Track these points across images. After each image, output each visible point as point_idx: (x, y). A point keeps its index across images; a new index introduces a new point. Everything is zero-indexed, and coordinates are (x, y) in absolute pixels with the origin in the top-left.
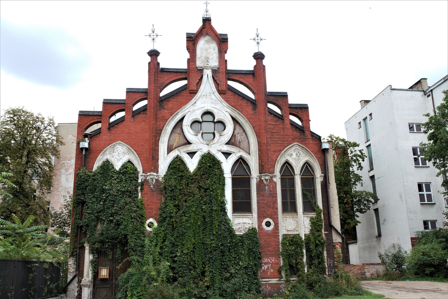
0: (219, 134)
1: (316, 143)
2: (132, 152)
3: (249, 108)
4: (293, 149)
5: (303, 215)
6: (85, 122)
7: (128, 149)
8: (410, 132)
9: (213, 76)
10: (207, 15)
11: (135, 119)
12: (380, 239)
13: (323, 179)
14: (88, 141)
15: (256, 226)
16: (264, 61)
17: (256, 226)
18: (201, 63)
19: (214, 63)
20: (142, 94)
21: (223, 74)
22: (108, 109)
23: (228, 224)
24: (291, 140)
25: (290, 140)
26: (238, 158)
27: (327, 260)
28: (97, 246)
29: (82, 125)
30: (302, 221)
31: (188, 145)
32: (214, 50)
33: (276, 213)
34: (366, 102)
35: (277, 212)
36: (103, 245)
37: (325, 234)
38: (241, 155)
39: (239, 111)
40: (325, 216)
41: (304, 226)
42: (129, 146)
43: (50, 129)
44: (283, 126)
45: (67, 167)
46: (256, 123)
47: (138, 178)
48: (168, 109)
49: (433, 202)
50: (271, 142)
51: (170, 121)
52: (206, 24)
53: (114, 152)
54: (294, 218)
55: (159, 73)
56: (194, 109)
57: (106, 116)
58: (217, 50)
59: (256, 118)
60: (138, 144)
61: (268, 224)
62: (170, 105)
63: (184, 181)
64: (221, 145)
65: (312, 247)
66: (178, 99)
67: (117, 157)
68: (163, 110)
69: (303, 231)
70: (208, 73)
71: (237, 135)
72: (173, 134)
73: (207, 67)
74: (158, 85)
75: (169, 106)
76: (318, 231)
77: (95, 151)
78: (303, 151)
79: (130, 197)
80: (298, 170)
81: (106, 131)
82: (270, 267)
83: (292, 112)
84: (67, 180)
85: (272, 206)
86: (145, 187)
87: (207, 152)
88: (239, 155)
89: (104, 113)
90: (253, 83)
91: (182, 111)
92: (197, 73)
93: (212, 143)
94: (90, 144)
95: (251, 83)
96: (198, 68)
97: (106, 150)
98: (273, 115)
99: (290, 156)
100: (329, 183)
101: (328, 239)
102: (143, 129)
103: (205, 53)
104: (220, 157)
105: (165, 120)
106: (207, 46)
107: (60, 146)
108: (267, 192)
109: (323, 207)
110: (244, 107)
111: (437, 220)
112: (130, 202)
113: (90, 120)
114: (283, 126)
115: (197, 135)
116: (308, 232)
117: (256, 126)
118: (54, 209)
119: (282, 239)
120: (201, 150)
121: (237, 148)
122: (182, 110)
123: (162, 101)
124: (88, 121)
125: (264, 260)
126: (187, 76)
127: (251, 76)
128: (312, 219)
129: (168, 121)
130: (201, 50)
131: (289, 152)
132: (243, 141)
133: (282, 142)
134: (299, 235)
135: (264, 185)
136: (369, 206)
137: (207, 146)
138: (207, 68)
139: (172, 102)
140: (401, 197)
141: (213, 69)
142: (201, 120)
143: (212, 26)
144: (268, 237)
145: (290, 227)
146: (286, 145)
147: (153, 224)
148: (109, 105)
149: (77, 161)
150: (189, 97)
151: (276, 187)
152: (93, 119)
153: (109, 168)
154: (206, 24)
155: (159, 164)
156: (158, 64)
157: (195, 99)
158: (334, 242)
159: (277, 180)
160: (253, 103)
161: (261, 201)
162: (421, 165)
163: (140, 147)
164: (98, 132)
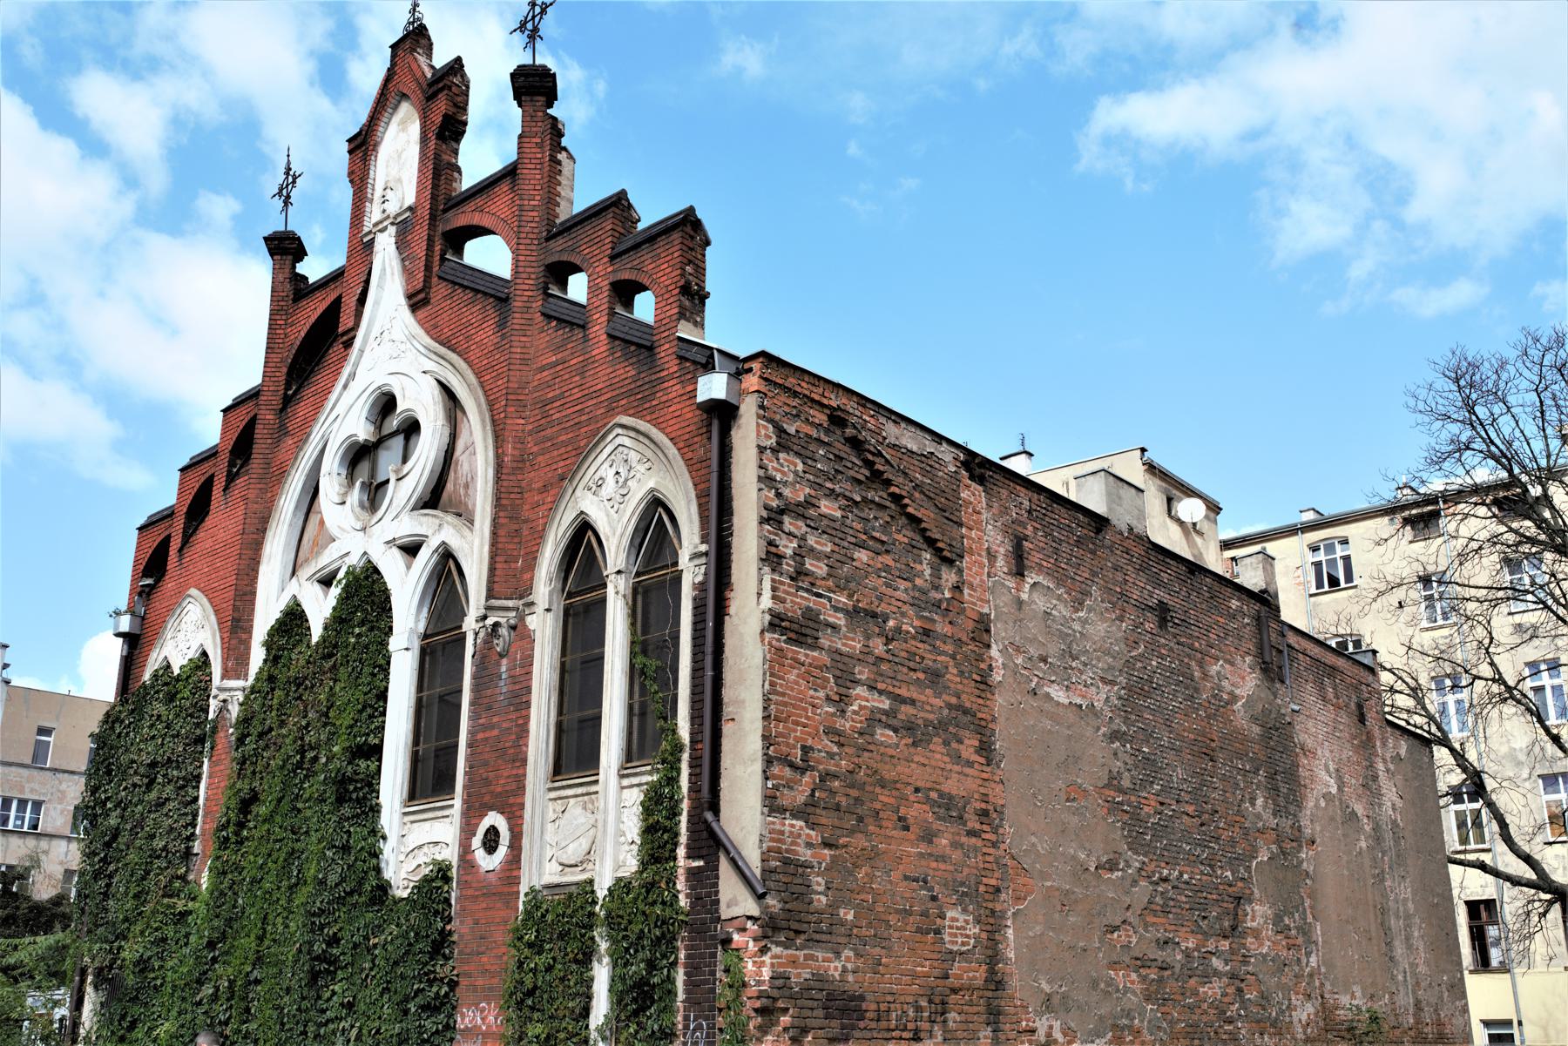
10: (413, 22)
15: (450, 854)
17: (450, 854)
24: (602, 411)
27: (686, 1018)
37: (692, 874)
70: (386, 245)
71: (461, 458)
78: (640, 447)
96: (365, 240)
101: (698, 898)
108: (504, 687)
114: (581, 359)
116: (631, 865)
133: (570, 436)
135: (498, 657)
137: (361, 533)
138: (380, 227)
141: (399, 219)
144: (484, 905)
158: (725, 913)
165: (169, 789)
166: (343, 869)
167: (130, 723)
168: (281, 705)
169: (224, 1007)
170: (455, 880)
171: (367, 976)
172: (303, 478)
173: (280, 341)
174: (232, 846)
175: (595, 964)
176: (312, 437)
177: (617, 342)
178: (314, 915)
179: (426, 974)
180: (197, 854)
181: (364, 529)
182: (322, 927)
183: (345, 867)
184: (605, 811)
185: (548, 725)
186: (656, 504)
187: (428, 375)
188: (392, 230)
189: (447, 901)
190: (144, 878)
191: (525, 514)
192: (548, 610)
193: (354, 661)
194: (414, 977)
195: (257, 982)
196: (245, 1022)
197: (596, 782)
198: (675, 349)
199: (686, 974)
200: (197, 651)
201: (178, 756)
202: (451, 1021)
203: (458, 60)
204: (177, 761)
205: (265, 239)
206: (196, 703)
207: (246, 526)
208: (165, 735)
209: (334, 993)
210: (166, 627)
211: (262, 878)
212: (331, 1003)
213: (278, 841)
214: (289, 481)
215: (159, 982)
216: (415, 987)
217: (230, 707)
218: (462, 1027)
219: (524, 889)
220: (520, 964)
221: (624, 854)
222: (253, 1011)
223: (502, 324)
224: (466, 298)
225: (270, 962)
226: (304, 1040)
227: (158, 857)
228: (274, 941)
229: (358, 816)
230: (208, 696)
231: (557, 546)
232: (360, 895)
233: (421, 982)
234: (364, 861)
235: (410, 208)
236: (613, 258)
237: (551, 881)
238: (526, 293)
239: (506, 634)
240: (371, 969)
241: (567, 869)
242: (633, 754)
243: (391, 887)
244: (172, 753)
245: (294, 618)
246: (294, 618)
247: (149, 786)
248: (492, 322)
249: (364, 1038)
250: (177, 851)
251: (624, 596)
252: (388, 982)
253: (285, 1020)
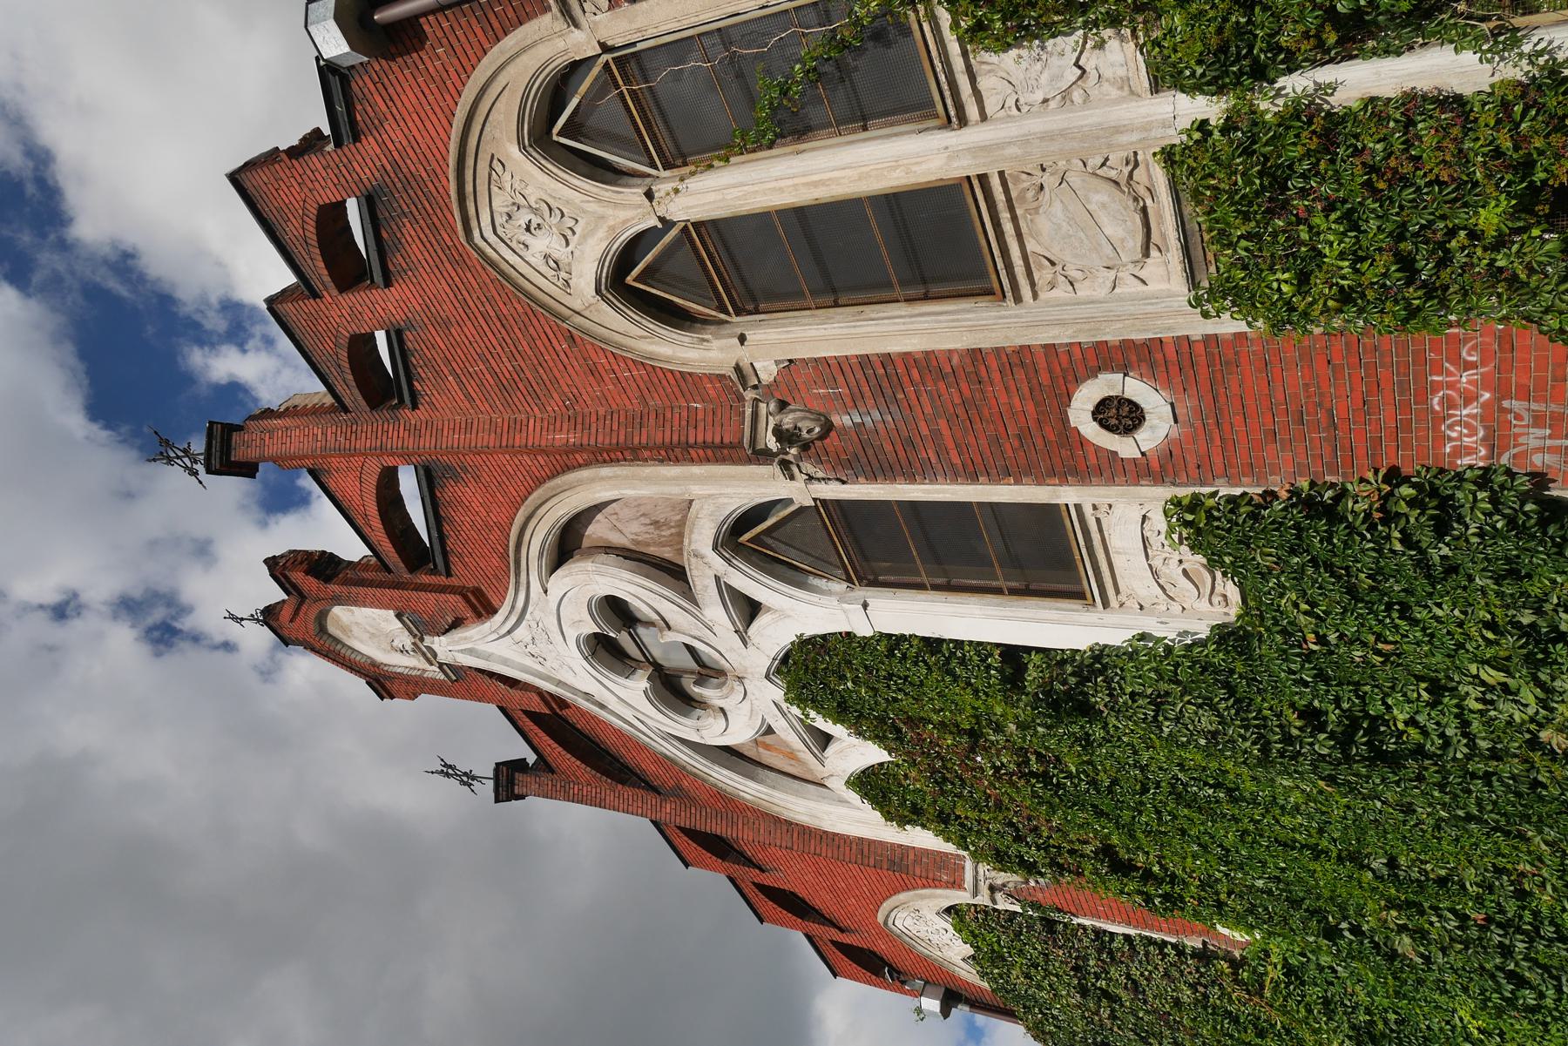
5: (963, 121)
9: (444, 634)
15: (1155, 497)
35: (998, 351)
38: (715, 548)
54: (1022, 197)
82: (1534, 406)
85: (963, 385)
88: (718, 564)
96: (454, 678)
98: (416, 383)
99: (563, 274)
108: (872, 417)
125: (1459, 452)
128: (976, 33)
135: (833, 434)
137: (745, 681)
138: (429, 655)
165: (1114, 972)
166: (1189, 702)
167: (1041, 1012)
168: (976, 806)
169: (1434, 919)
170: (1198, 490)
171: (1378, 653)
172: (716, 768)
173: (594, 790)
174: (1177, 889)
175: (1340, 100)
176: (667, 753)
177: (391, 267)
178: (1265, 750)
179: (1372, 528)
180: (1204, 943)
181: (740, 679)
182: (1288, 739)
183: (1187, 698)
184: (1025, 141)
185: (911, 316)
187: (549, 586)
188: (428, 640)
189: (1231, 500)
190: (1235, 1020)
191: (635, 406)
192: (742, 339)
193: (889, 687)
194: (1379, 551)
195: (1392, 863)
196: (1463, 887)
197: (983, 178)
198: (351, 146)
201: (1070, 956)
202: (1468, 474)
203: (266, 561)
204: (1077, 958)
205: (497, 801)
206: (1002, 926)
207: (784, 845)
208: (1045, 970)
209: (1411, 722)
210: (928, 956)
211: (1221, 846)
212: (1431, 726)
213: (1160, 819)
214: (724, 786)
215: (1392, 1017)
216: (1398, 547)
218: (1483, 452)
219: (1197, 327)
220: (1345, 297)
221: (1106, 86)
222: (1443, 872)
224: (452, 533)
225: (1358, 840)
226: (1500, 779)
227: (1205, 996)
228: (1321, 831)
229: (1108, 681)
230: (995, 910)
231: (653, 334)
232: (1232, 672)
233: (1388, 538)
234: (1177, 665)
235: (399, 616)
236: (315, 295)
237: (1180, 267)
238: (401, 435)
239: (791, 416)
240: (1364, 644)
241: (1155, 237)
243: (1224, 626)
244: (1067, 963)
245: (869, 784)
246: (869, 784)
247: (1113, 999)
248: (456, 488)
249: (1503, 654)
250: (1198, 971)
251: (682, 180)
252: (1389, 607)
253: (1461, 813)
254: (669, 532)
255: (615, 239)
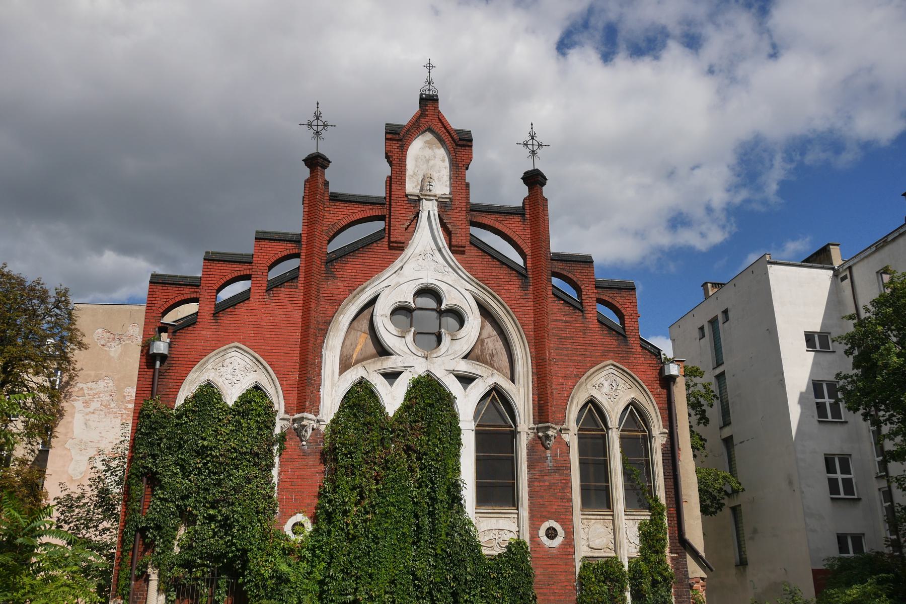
0: (451, 335)
1: (650, 362)
2: (264, 367)
3: (514, 286)
4: (605, 373)
5: (625, 515)
6: (162, 300)
7: (254, 360)
8: (807, 351)
9: (439, 215)
11: (273, 298)
12: (745, 570)
13: (665, 439)
14: (168, 340)
15: (526, 538)
16: (546, 191)
18: (416, 186)
19: (442, 187)
20: (290, 245)
21: (462, 212)
22: (214, 273)
23: (468, 532)
25: (597, 354)
26: (489, 389)
28: (178, 572)
29: (156, 305)
30: (623, 529)
31: (383, 357)
32: (443, 161)
33: (569, 511)
34: (716, 287)
36: (190, 572)
37: (672, 558)
38: (495, 383)
39: (492, 289)
40: (672, 519)
41: (627, 541)
42: (256, 355)
43: (57, 315)
44: (583, 325)
45: (87, 397)
46: (528, 316)
47: (274, 424)
48: (343, 279)
49: (856, 497)
50: (557, 357)
51: (348, 304)
52: (427, 108)
53: (223, 366)
54: (606, 523)
55: (328, 204)
56: (399, 283)
57: (210, 288)
58: (447, 163)
59: (527, 305)
60: (277, 351)
61: (551, 534)
62: (348, 271)
63: (375, 435)
64: (453, 359)
65: (646, 586)
66: (366, 258)
67: (230, 377)
68: (333, 282)
69: (626, 551)
70: (429, 208)
71: (486, 340)
72: (352, 333)
73: (429, 196)
74: (324, 228)
75: (347, 274)
76: (657, 552)
77: (183, 362)
79: (255, 464)
80: (614, 417)
81: (209, 321)
83: (602, 297)
84: (86, 424)
85: (560, 494)
86: (290, 444)
87: (424, 373)
88: (491, 381)
89: (205, 282)
90: (522, 233)
91: (373, 285)
92: (407, 207)
93: (435, 355)
94: (173, 346)
95: (517, 233)
96: (410, 197)
97: (208, 360)
98: (562, 302)
99: (597, 387)
100: (679, 449)
102: (289, 319)
103: (424, 167)
104: (453, 386)
105: (337, 303)
106: (428, 152)
107: (76, 352)
108: (549, 462)
109: (666, 500)
110: (503, 283)
111: (864, 534)
112: (256, 477)
113: (173, 294)
114: (583, 325)
115: (404, 337)
117: (527, 322)
118: (66, 488)
119: (581, 568)
120: (409, 369)
121: (487, 366)
122: (373, 282)
123: (332, 261)
124: (171, 297)
126: (385, 212)
127: (517, 219)
129: (342, 305)
130: (416, 161)
131: (596, 379)
132: (499, 354)
133: (580, 359)
134: (616, 558)
135: (544, 449)
136: (722, 501)
137: (425, 360)
138: (428, 197)
139: (353, 266)
140: (791, 483)
141: (440, 200)
142: (413, 305)
143: (439, 112)
145: (597, 542)
146: (589, 365)
147: (302, 525)
148: (217, 265)
149: (141, 382)
150: (389, 257)
151: (568, 454)
152: (181, 292)
153: (213, 401)
154: (427, 108)
155: (322, 396)
156: (326, 184)
157: (401, 261)
159: (572, 438)
160: (521, 274)
161: (536, 484)
162: (830, 419)
163: (282, 358)
164: (190, 322)
177: (604, 326)
186: (633, 403)
199: (675, 598)
200: (250, 385)
217: (308, 430)
223: (524, 287)
242: (628, 504)
254: (488, 358)
255: (607, 411)
